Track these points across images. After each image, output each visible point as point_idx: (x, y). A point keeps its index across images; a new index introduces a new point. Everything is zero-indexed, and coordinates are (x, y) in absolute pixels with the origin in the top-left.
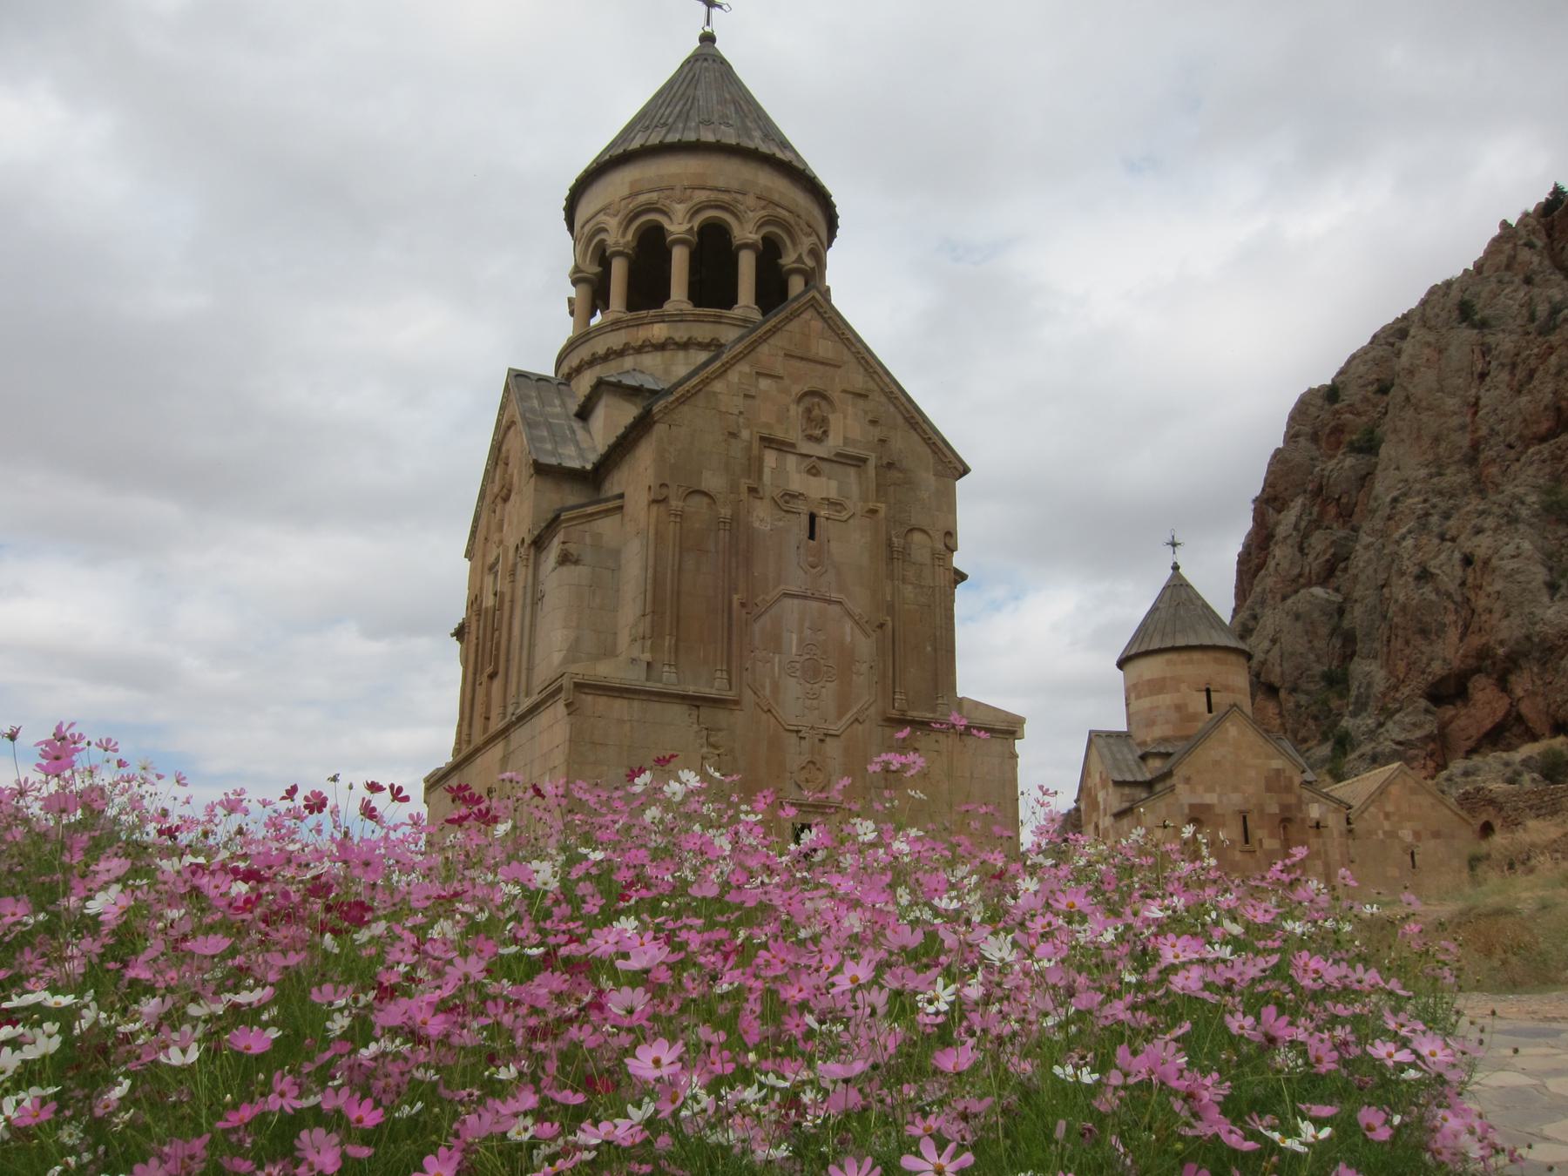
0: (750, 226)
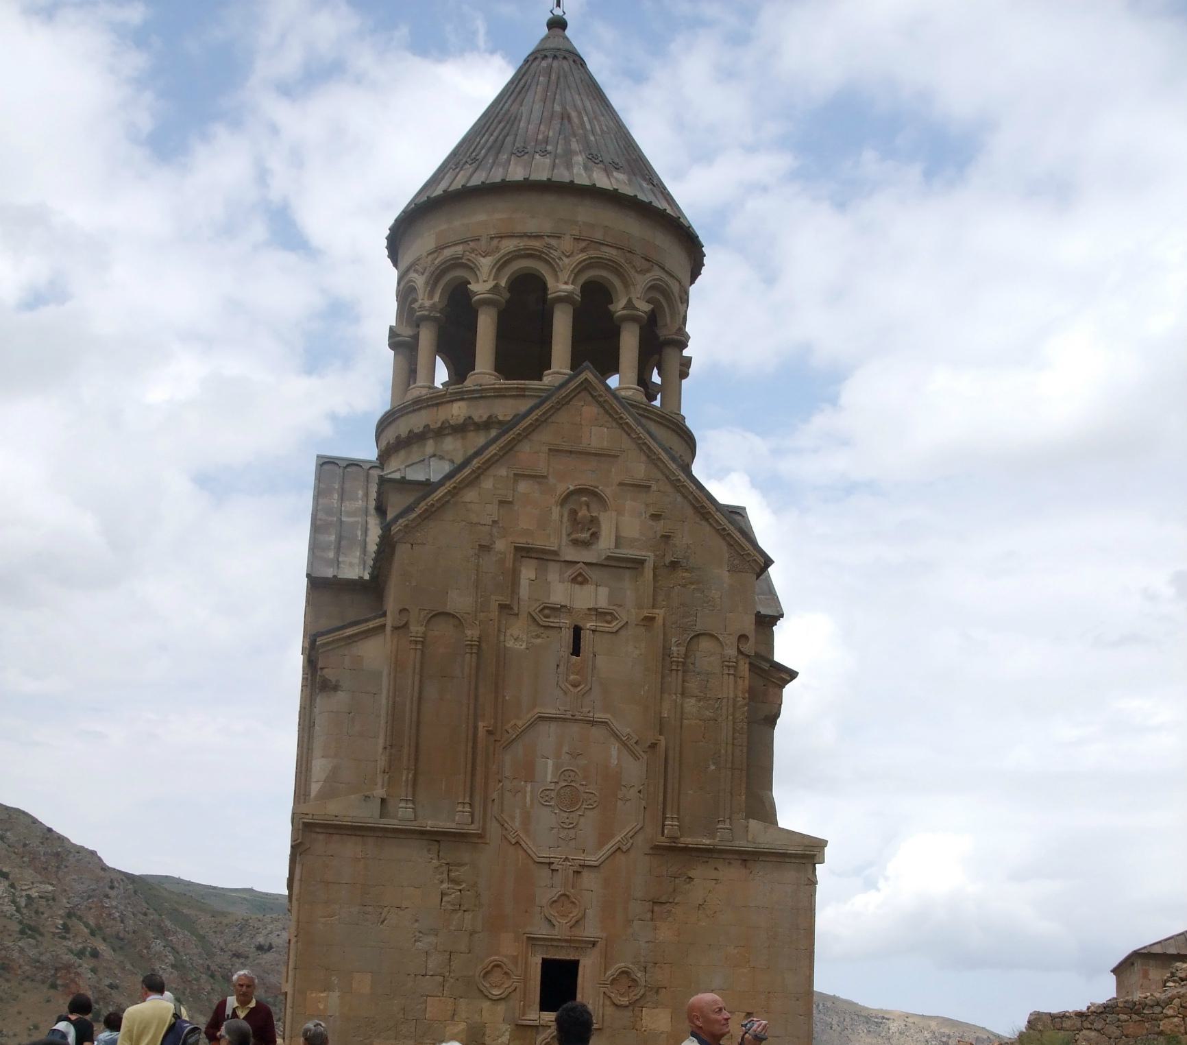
0: (564, 276)
